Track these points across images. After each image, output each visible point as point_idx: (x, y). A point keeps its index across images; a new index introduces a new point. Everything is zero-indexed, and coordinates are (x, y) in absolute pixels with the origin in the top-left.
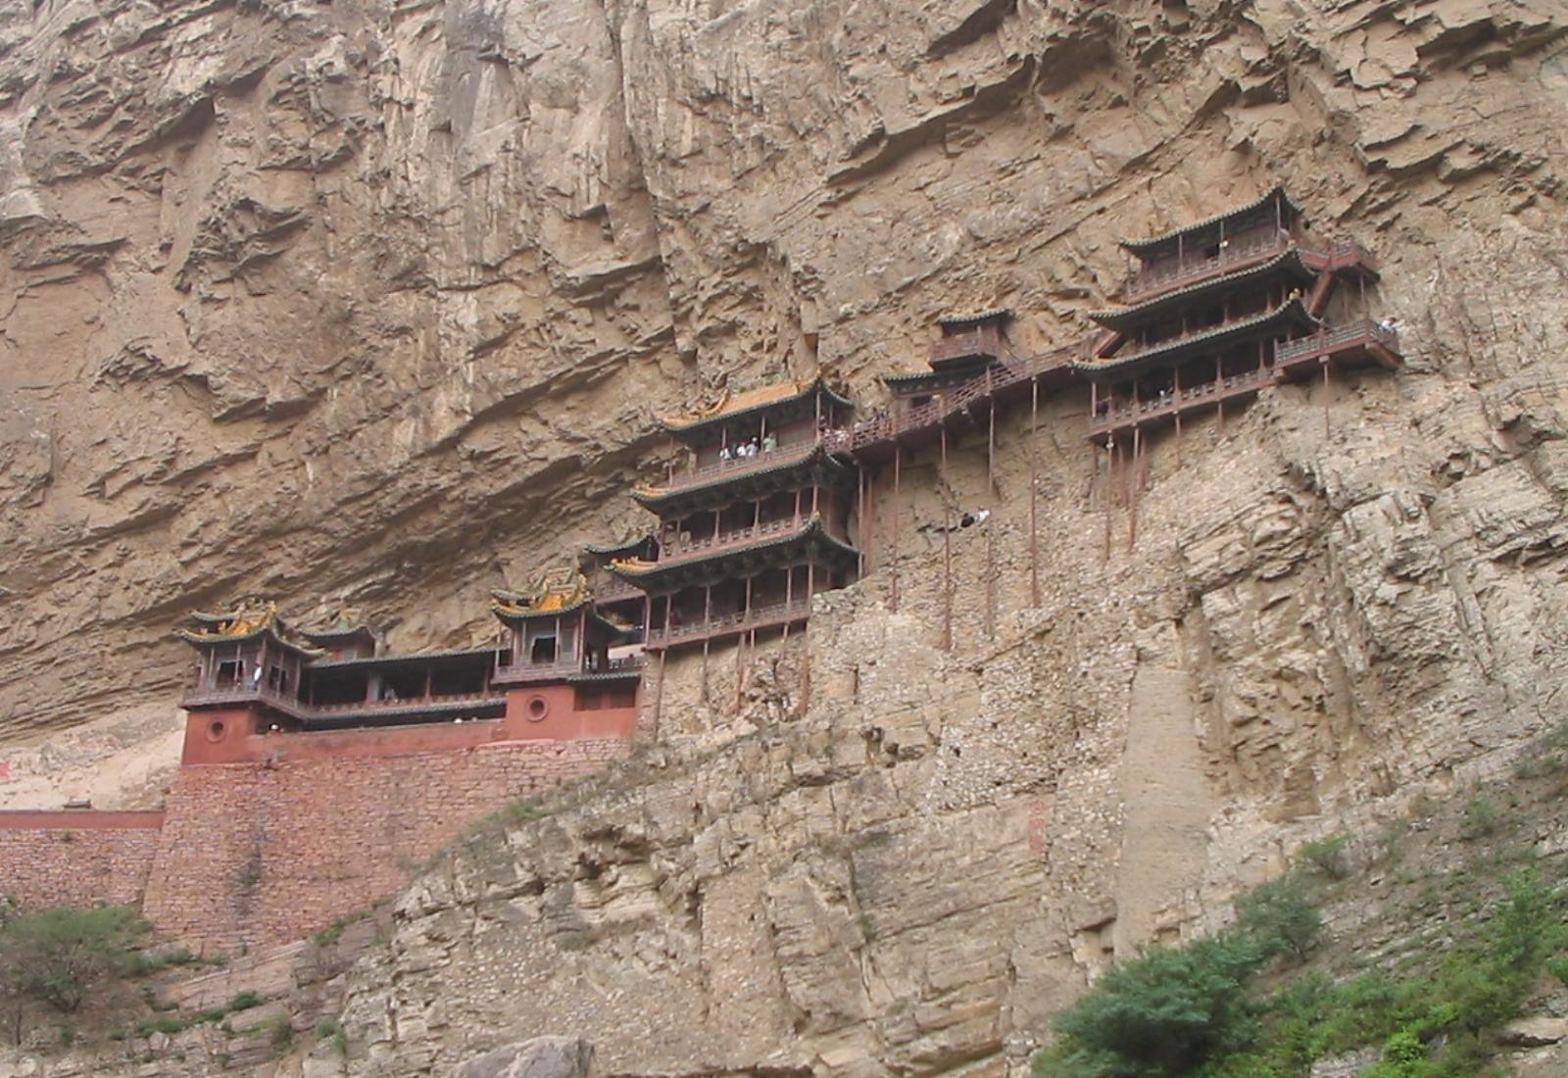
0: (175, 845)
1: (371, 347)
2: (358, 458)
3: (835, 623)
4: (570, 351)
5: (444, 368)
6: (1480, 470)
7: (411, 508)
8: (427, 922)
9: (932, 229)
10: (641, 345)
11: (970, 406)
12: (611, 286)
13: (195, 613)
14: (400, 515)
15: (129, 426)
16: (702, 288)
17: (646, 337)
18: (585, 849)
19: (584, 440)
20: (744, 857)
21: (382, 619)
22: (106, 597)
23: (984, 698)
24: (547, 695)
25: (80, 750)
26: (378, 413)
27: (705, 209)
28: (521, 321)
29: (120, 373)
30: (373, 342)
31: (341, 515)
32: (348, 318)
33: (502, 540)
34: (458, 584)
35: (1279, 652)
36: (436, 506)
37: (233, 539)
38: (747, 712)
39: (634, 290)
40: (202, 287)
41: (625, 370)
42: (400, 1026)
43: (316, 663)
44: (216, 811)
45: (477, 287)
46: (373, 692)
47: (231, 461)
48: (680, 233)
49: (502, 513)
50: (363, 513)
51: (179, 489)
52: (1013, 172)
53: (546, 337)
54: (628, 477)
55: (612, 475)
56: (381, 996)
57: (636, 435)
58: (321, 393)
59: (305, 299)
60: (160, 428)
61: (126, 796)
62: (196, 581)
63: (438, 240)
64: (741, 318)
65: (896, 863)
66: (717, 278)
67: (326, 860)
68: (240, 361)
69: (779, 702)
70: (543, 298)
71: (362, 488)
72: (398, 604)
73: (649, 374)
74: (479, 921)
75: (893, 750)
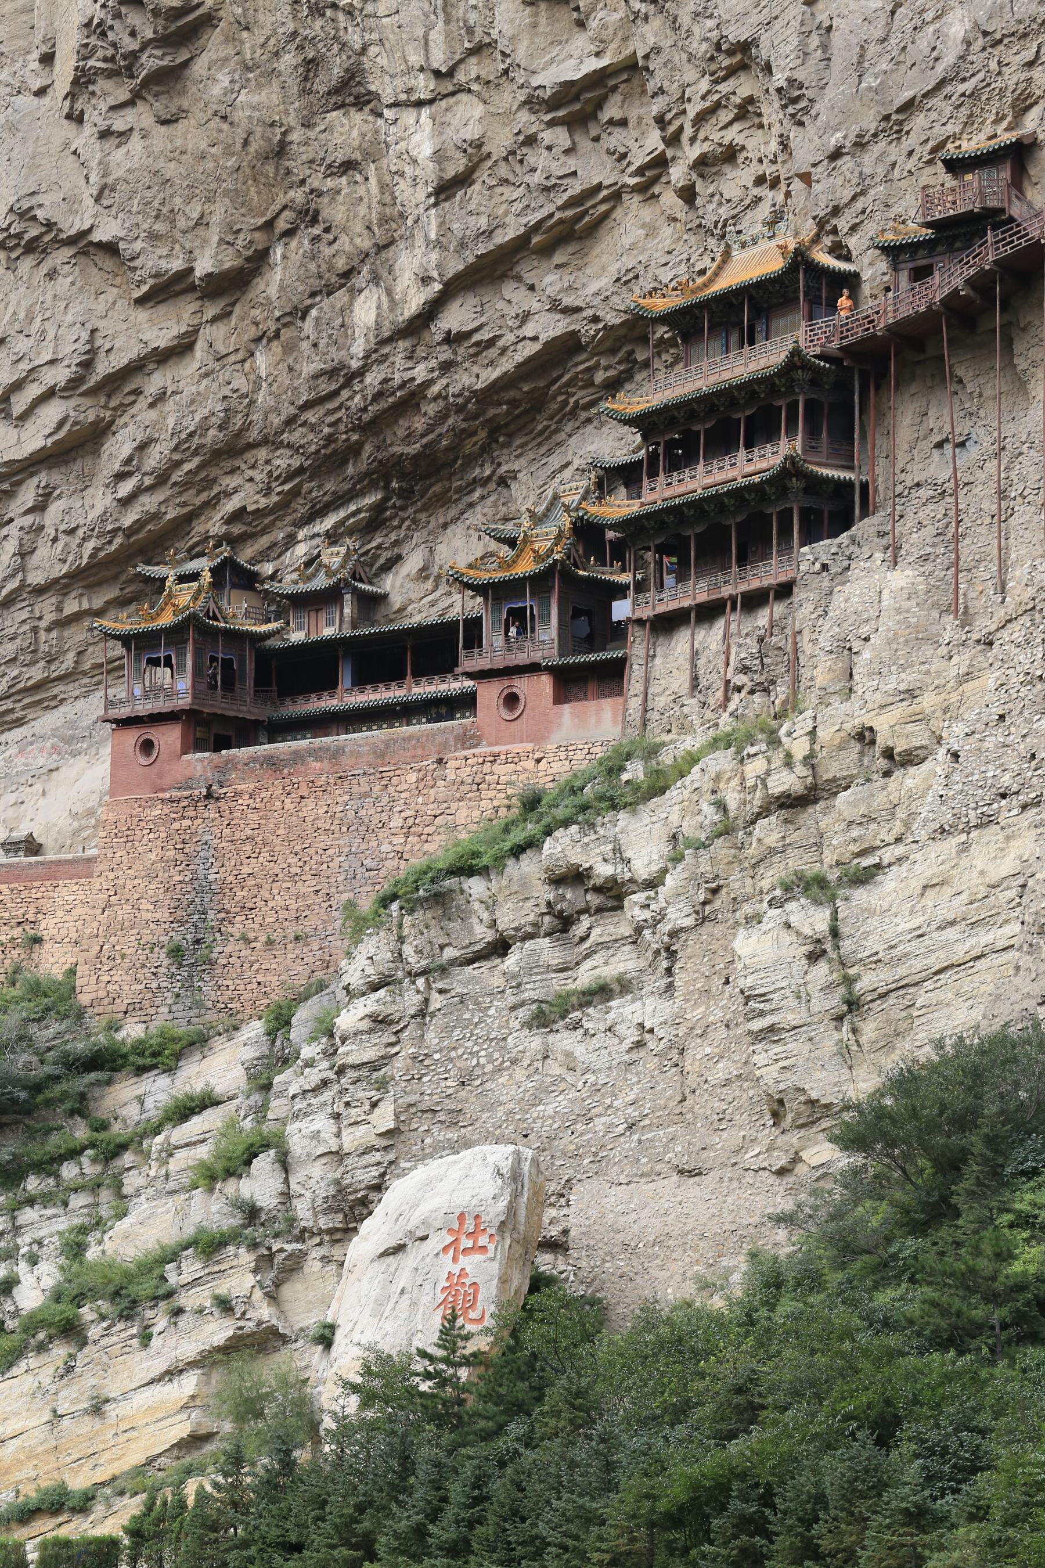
0: (108, 905)
1: (312, 191)
2: (315, 345)
3: (826, 583)
4: (547, 189)
5: (403, 216)
7: (385, 411)
8: (369, 1004)
9: (938, 17)
10: (632, 175)
11: (968, 282)
12: (589, 95)
13: (142, 568)
14: (374, 421)
15: (31, 320)
16: (689, 100)
17: (638, 164)
18: (551, 896)
19: (578, 310)
20: (717, 904)
21: (375, 557)
22: (32, 552)
23: (990, 680)
24: (522, 685)
25: (20, 761)
26: (334, 279)
28: (485, 149)
29: (12, 243)
30: (315, 182)
31: (304, 424)
32: (281, 150)
33: (504, 446)
34: (461, 505)
36: (418, 405)
37: (178, 464)
38: (732, 707)
39: (616, 99)
40: (96, 115)
41: (618, 214)
42: (344, 1133)
43: (274, 643)
44: (153, 856)
45: (431, 102)
46: (346, 678)
47: (164, 357)
48: (656, 22)
49: (498, 411)
50: (331, 419)
51: (103, 400)
53: (518, 168)
54: (640, 356)
55: (621, 355)
56: (327, 1095)
58: (259, 260)
59: (225, 126)
60: (69, 318)
61: (76, 824)
62: (138, 525)
63: (375, 36)
64: (739, 140)
65: (885, 907)
66: (704, 85)
67: (283, 914)
68: (157, 217)
69: (766, 690)
70: (509, 115)
71: (326, 387)
72: (393, 537)
73: (647, 213)
74: (435, 996)
75: (888, 753)
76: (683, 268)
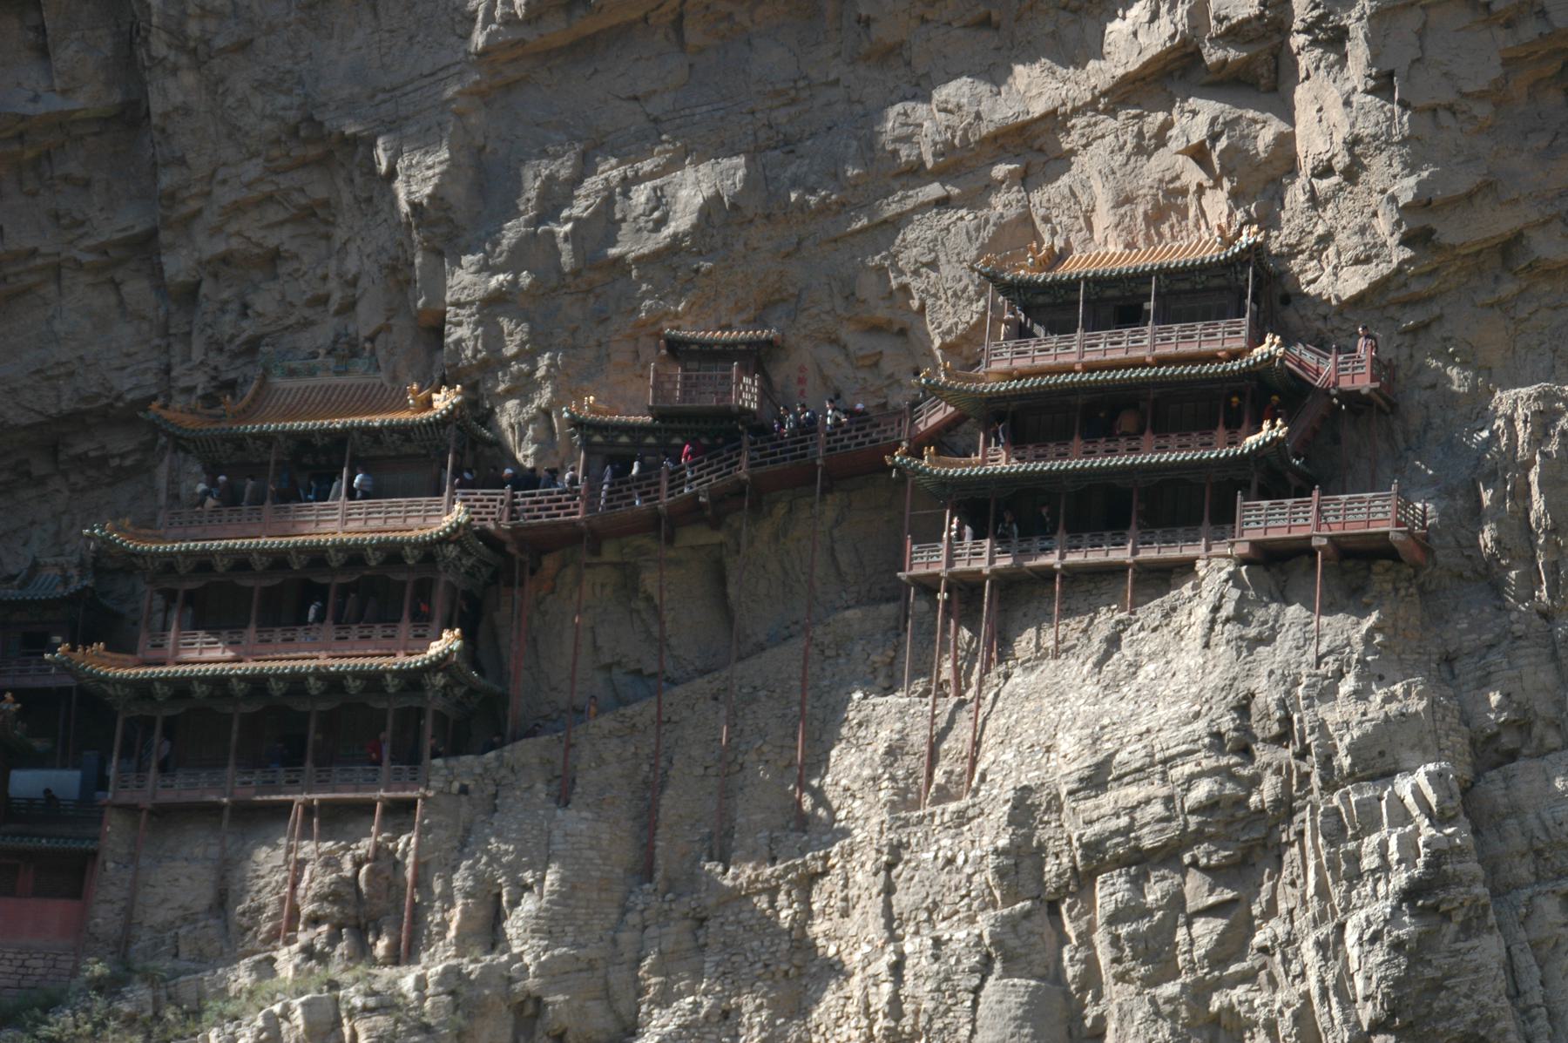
6: (1541, 753)
27: (244, 46)
35: (1219, 985)
48: (188, 79)
52: (793, 102)
57: (66, 406)
64: (290, 246)
76: (150, 378)
